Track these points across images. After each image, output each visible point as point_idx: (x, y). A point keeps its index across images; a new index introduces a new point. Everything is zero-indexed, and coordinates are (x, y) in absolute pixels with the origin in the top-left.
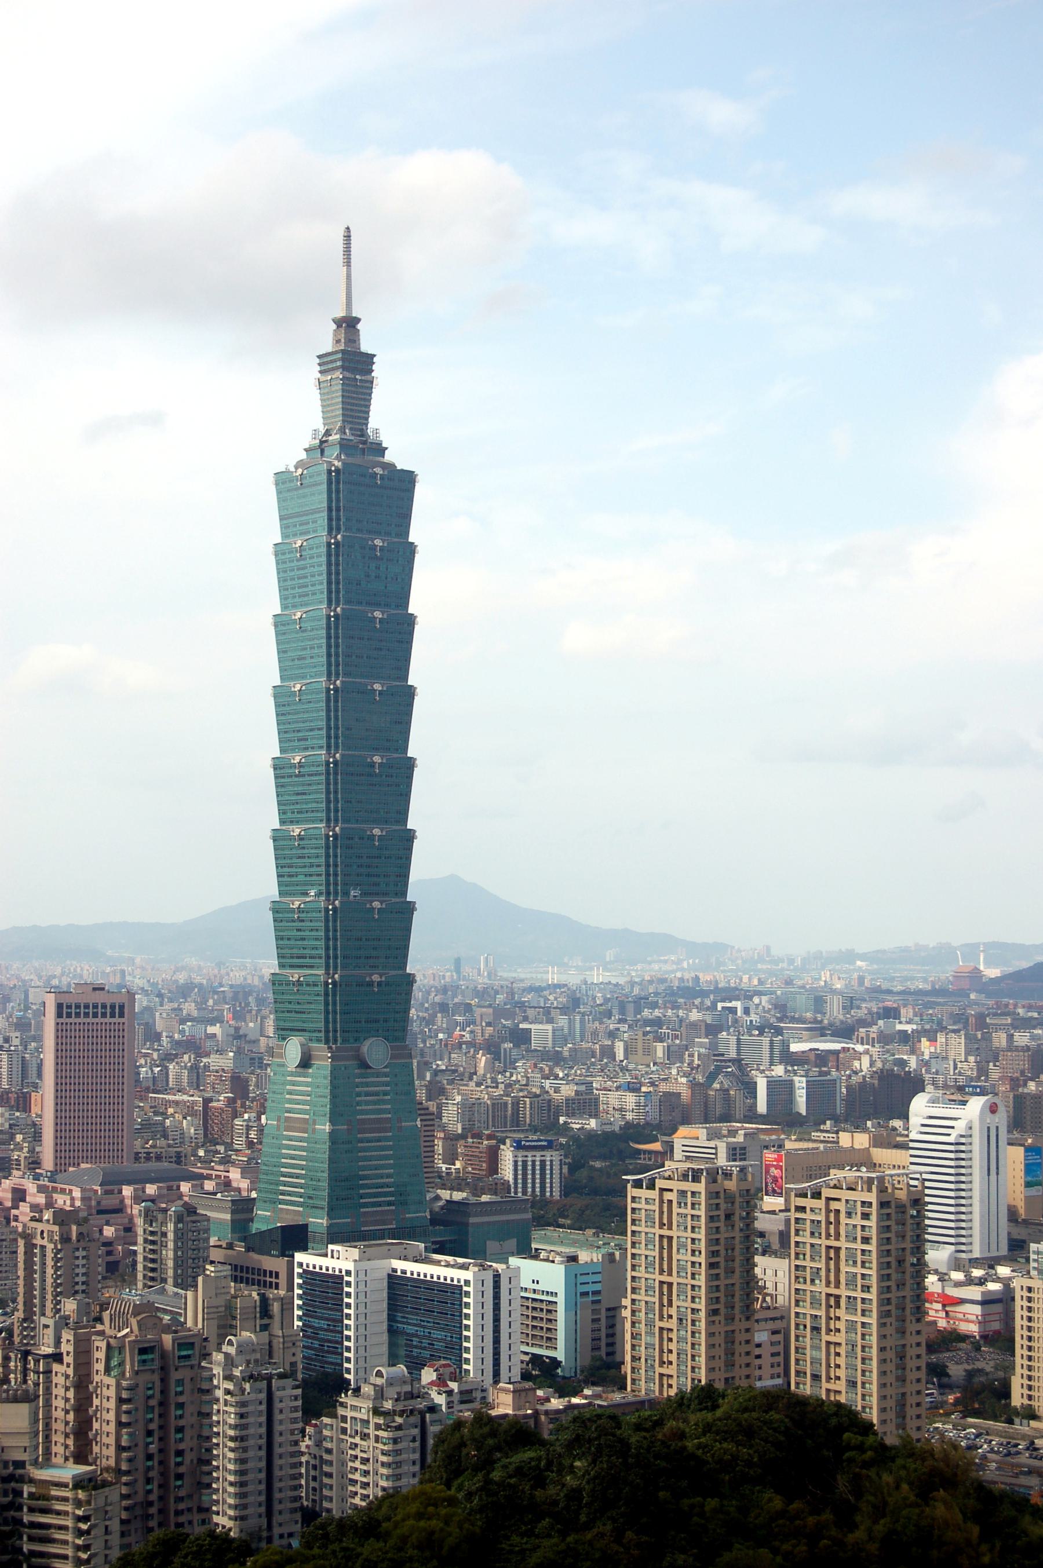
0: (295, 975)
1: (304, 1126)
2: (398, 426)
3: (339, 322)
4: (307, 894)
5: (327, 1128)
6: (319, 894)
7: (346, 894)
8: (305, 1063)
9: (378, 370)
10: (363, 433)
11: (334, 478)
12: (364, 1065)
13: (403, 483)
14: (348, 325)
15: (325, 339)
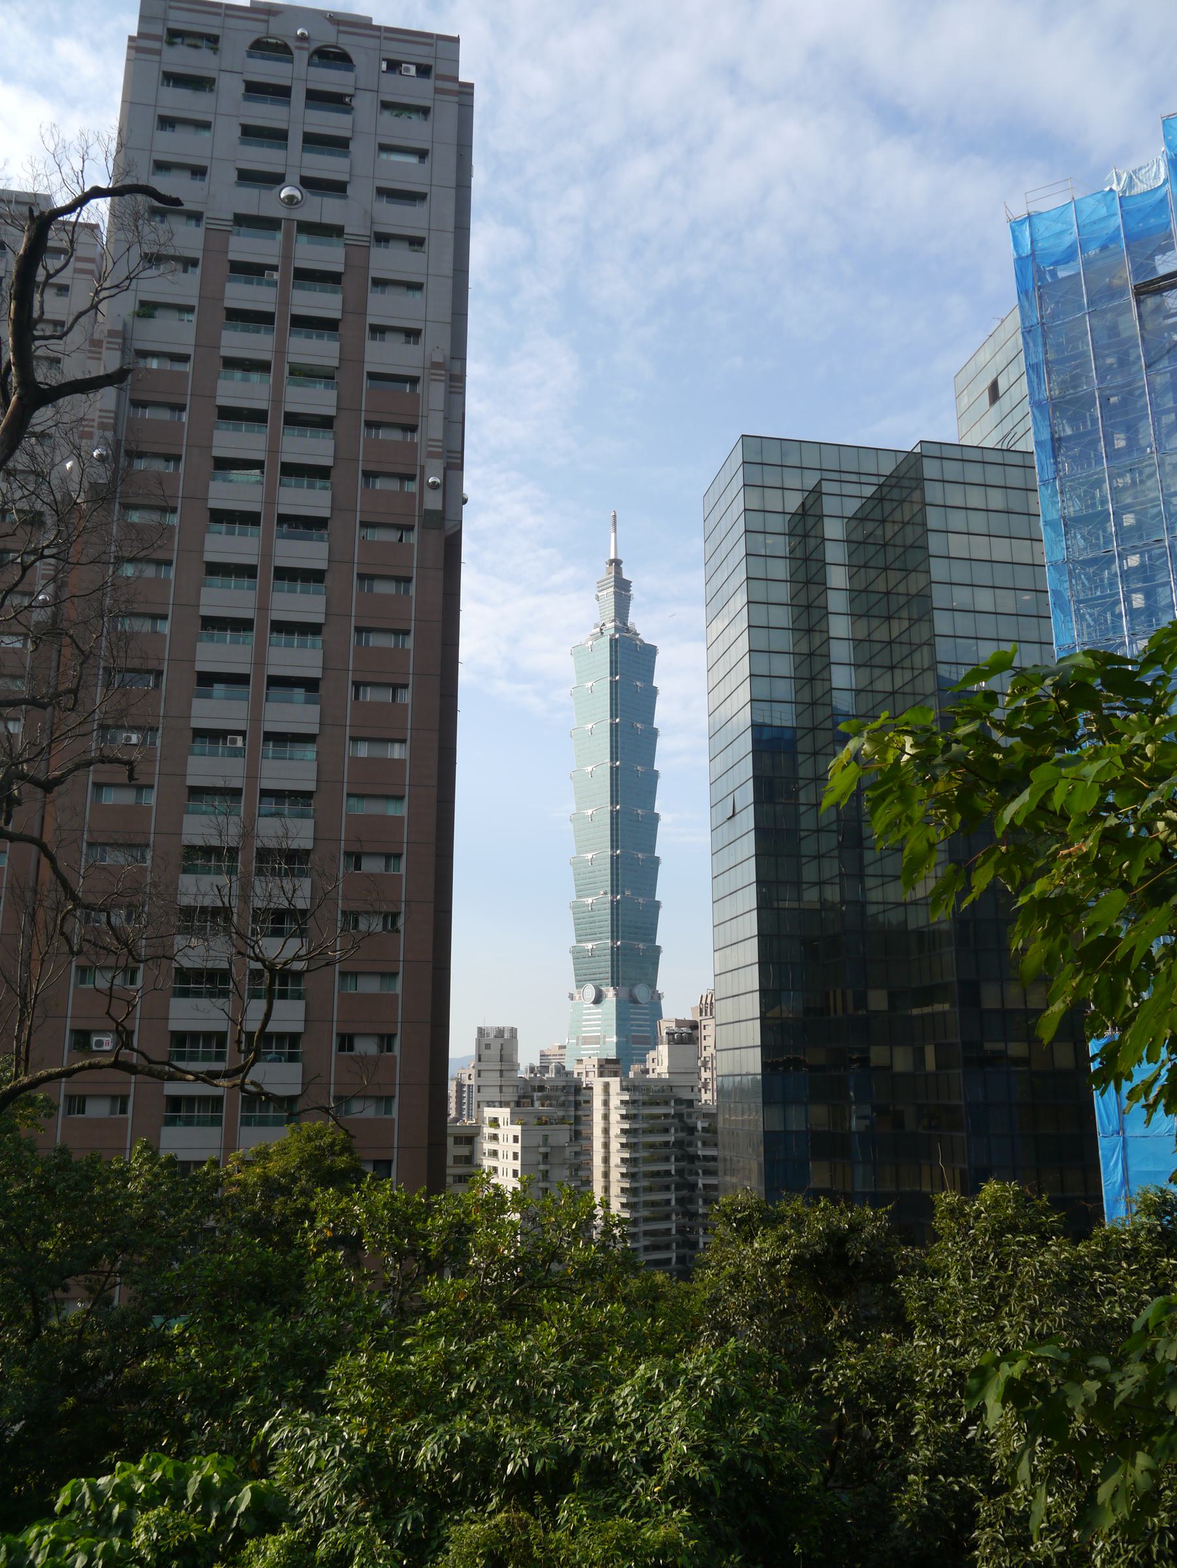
0: (589, 946)
1: (595, 1040)
2: (645, 624)
3: (611, 562)
4: (598, 894)
5: (614, 1039)
6: (605, 893)
7: (623, 893)
8: (598, 1000)
9: (634, 591)
10: (625, 624)
11: (614, 643)
12: (634, 1001)
13: (651, 651)
14: (617, 563)
15: (605, 573)
